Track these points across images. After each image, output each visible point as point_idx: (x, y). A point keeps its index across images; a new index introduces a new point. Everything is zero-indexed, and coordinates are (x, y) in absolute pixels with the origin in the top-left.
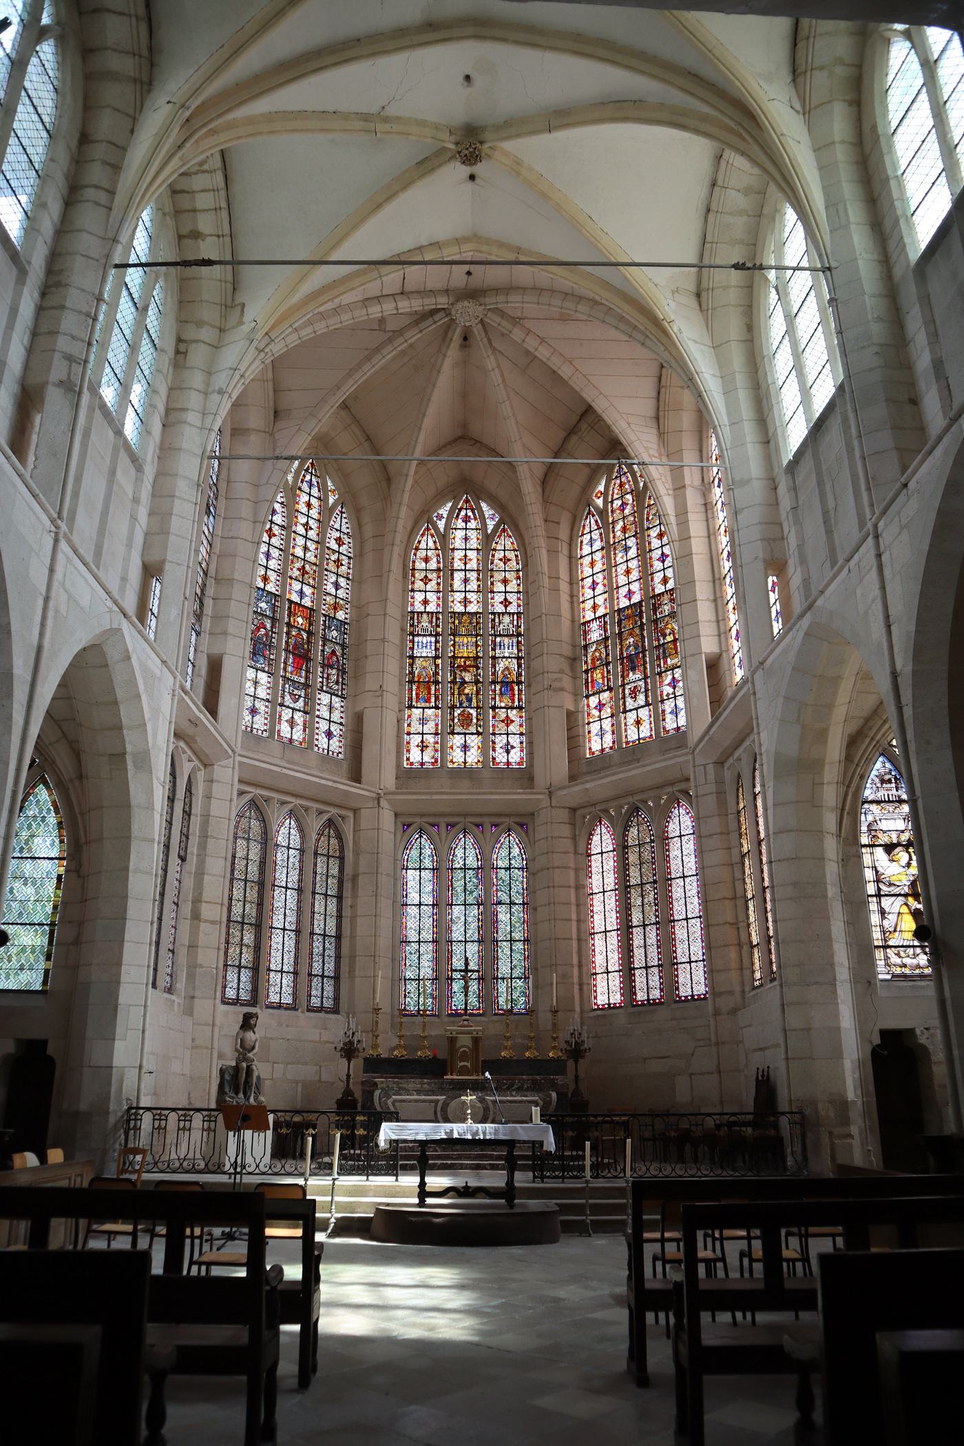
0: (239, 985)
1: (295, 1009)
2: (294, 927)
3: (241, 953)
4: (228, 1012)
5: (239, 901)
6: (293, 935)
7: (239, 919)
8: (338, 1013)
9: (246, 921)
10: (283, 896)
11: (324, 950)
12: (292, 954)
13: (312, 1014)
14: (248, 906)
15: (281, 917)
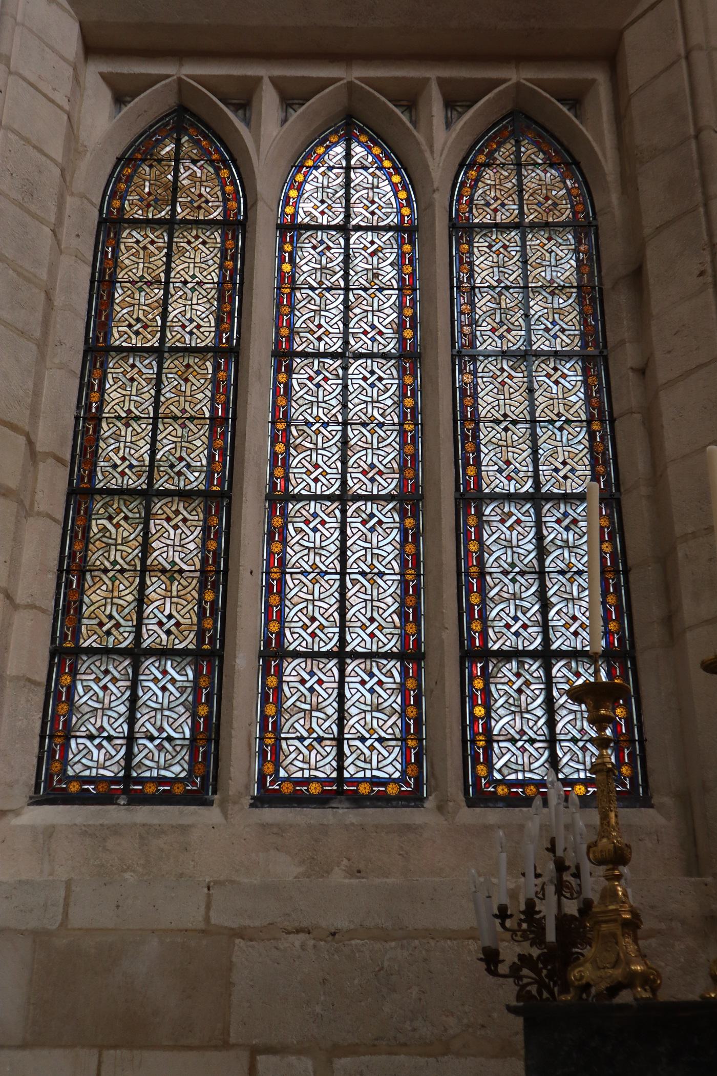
0: (132, 720)
1: (414, 799)
2: (389, 485)
3: (141, 600)
4: (50, 832)
5: (129, 419)
6: (387, 514)
7: (132, 481)
8: (646, 802)
9: (161, 483)
10: (334, 386)
11: (542, 552)
12: (390, 586)
13: (492, 815)
14: (168, 435)
15: (329, 457)
